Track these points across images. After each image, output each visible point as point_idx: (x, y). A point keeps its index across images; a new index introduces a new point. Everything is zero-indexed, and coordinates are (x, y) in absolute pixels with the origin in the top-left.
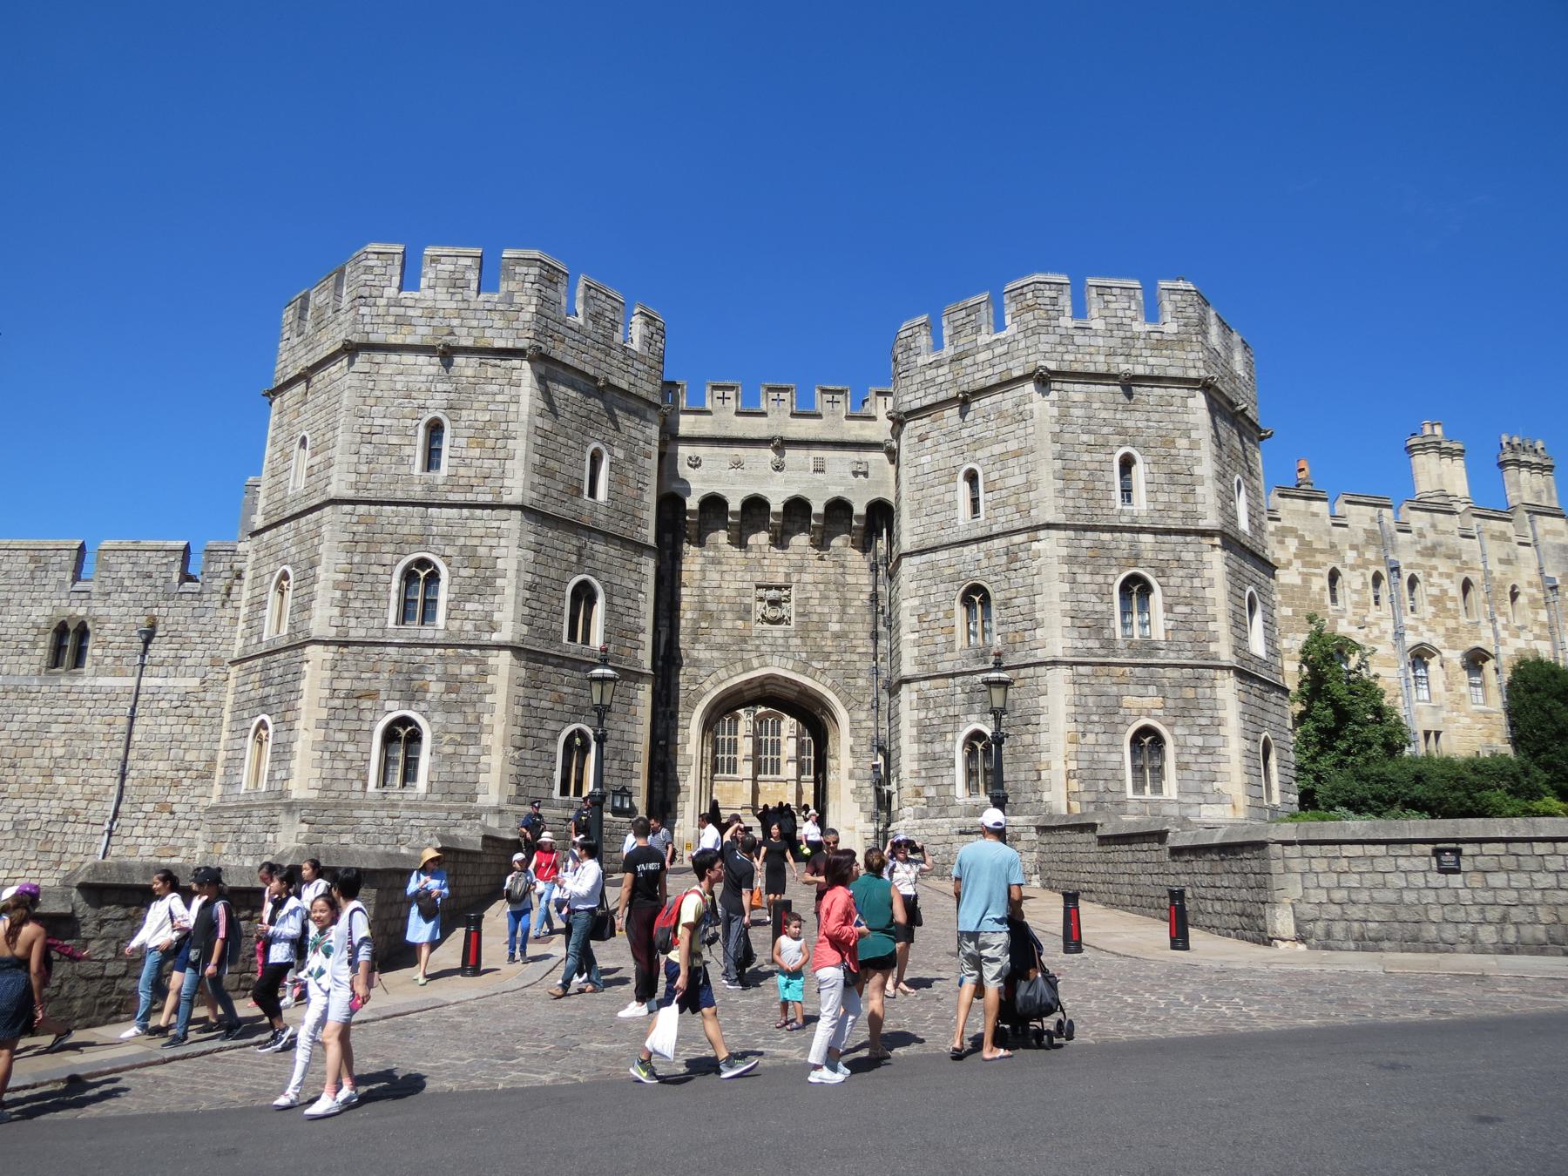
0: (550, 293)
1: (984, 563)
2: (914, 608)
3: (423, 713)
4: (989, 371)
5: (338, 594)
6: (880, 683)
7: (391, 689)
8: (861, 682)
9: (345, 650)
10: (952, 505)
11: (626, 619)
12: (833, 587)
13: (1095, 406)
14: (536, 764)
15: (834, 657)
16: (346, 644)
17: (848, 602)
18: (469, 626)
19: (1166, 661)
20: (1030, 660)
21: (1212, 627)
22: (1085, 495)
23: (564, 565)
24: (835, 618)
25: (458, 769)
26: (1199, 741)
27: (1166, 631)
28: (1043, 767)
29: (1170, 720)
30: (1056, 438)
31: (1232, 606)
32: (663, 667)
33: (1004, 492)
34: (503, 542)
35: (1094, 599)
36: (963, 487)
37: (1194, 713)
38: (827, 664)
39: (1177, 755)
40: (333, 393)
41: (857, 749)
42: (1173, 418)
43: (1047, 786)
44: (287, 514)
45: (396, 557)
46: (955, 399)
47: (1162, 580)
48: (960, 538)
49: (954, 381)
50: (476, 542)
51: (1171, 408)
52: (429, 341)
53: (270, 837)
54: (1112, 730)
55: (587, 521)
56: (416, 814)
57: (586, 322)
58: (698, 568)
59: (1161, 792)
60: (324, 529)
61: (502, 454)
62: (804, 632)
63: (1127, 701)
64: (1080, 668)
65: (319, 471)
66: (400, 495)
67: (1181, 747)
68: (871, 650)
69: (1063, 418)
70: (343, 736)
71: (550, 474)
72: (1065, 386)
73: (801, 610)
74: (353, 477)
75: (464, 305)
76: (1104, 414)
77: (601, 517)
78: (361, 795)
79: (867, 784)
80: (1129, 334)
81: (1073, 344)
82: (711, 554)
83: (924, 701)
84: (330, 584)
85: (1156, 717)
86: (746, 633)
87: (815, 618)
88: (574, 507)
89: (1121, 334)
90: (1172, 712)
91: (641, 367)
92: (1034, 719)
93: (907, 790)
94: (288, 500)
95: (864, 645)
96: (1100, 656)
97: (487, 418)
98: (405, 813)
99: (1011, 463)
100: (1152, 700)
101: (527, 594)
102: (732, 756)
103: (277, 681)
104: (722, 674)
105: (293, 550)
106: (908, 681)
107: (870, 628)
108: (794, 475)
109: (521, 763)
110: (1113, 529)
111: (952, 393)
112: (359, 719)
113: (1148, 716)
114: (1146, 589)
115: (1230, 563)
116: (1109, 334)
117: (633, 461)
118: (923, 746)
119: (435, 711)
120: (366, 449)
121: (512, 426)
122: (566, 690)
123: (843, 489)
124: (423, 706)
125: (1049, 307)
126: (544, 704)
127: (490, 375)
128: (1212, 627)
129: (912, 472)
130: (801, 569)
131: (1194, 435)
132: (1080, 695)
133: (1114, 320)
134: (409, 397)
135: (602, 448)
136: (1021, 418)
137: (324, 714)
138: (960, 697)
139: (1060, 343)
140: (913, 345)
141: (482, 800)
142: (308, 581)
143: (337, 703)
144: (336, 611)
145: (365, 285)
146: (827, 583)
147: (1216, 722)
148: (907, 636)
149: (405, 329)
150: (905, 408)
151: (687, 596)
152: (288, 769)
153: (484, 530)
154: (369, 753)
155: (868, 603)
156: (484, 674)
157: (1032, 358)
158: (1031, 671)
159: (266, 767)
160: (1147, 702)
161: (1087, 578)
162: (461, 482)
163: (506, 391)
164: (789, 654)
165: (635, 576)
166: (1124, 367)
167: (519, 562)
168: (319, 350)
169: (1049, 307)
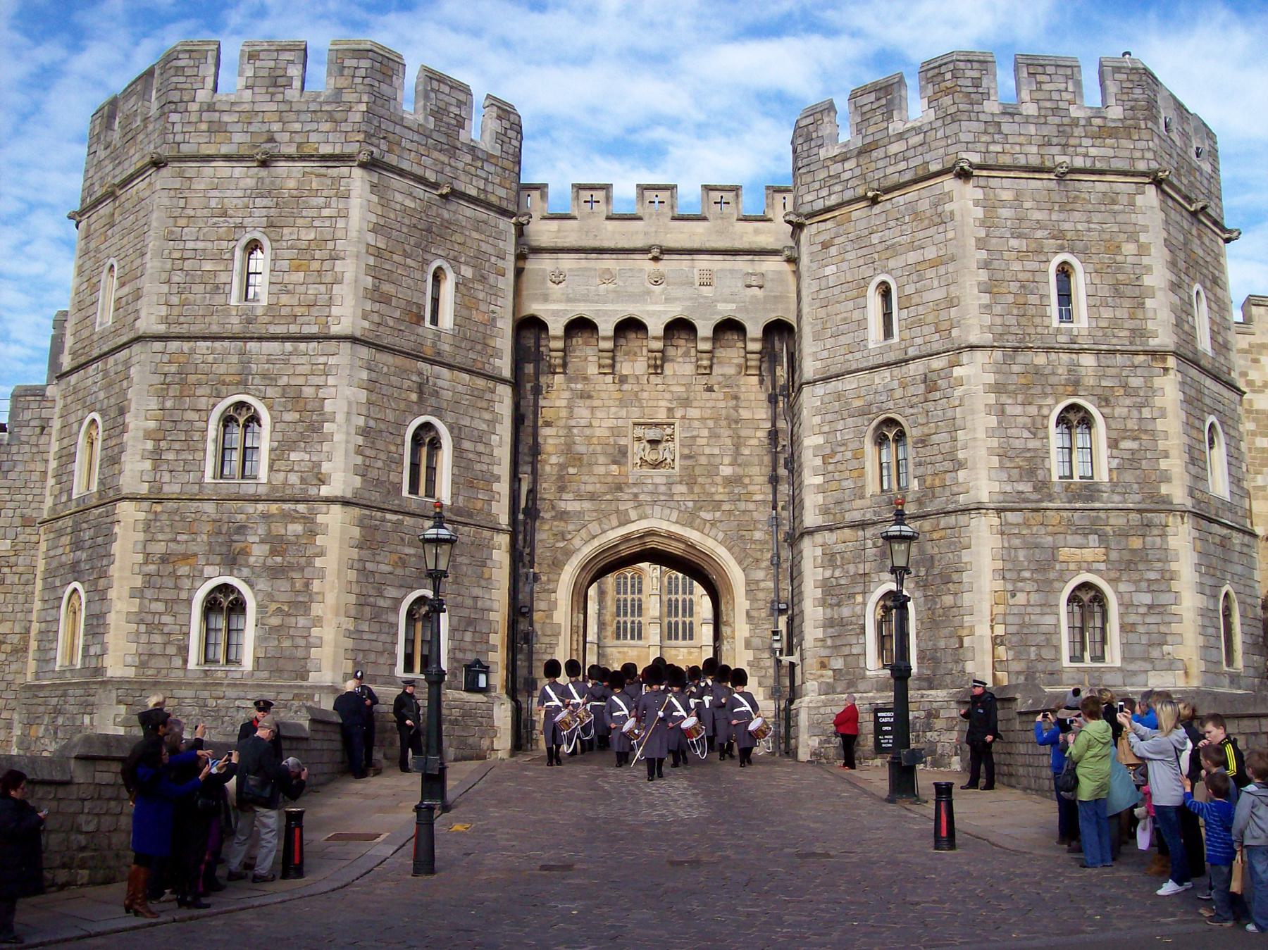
0: (385, 88)
1: (898, 393)
2: (817, 447)
3: (246, 581)
4: (902, 165)
5: (149, 445)
6: (781, 537)
7: (211, 551)
8: (758, 535)
9: (158, 508)
10: (862, 324)
11: (478, 467)
12: (724, 423)
13: (1026, 205)
14: (374, 637)
15: (726, 507)
16: (160, 501)
17: (742, 440)
18: (294, 478)
19: (1110, 506)
20: (951, 507)
21: (1163, 464)
22: (1015, 312)
23: (403, 405)
24: (727, 460)
25: (287, 643)
26: (1146, 599)
27: (1110, 470)
28: (965, 632)
29: (1113, 575)
30: (981, 244)
31: (1186, 440)
32: (525, 520)
33: (920, 308)
34: (331, 381)
35: (1026, 434)
36: (874, 302)
37: (1141, 566)
38: (718, 514)
39: (1121, 615)
40: (142, 213)
41: (754, 613)
42: (1120, 218)
43: (970, 655)
44: (95, 353)
45: (212, 401)
46: (864, 198)
47: (1106, 410)
48: (870, 364)
49: (863, 176)
50: (301, 381)
51: (1116, 207)
52: (244, 151)
53: (87, 719)
54: (1047, 587)
55: (429, 352)
56: (242, 694)
57: (426, 119)
58: (563, 403)
59: (1102, 658)
60: (133, 370)
61: (328, 278)
62: (690, 480)
63: (1064, 553)
64: (1009, 514)
65: (128, 304)
66: (215, 329)
67: (1126, 606)
68: (770, 498)
69: (988, 222)
70: (159, 607)
71: (385, 299)
72: (993, 182)
73: (686, 452)
74: (164, 311)
75: (287, 107)
76: (1038, 215)
77: (446, 348)
78: (181, 673)
79: (766, 655)
80: (1066, 121)
81: (1000, 132)
82: (579, 386)
83: (830, 558)
84: (141, 434)
85: (1097, 572)
86: (622, 480)
87: (703, 460)
88: (412, 338)
89: (1057, 120)
90: (1117, 565)
91: (492, 169)
92: (955, 577)
93: (811, 662)
94: (95, 337)
95: (761, 491)
96: (1033, 501)
97: (312, 236)
98: (231, 693)
99: (930, 273)
100: (1093, 552)
101: (360, 440)
102: (637, 619)
103: (87, 544)
104: (594, 528)
106: (811, 532)
107: (767, 470)
108: (677, 292)
109: (356, 634)
110: (1048, 350)
111: (860, 191)
112: (176, 587)
113: (1089, 571)
115: (1187, 390)
116: (1043, 120)
117: (483, 279)
118: (828, 611)
119: (259, 576)
120: (178, 277)
123: (733, 306)
124: (246, 572)
125: (971, 90)
126: (385, 568)
127: (314, 186)
128: (1163, 464)
130: (686, 402)
131: (1143, 238)
132: (1010, 547)
133: (1048, 104)
134: (224, 214)
135: (445, 265)
136: (941, 220)
137: (138, 582)
139: (985, 132)
140: (814, 135)
141: (314, 678)
142: (118, 431)
143: (152, 568)
144: (148, 465)
145: (176, 89)
146: (716, 420)
147: (1167, 576)
148: (811, 479)
149: (220, 137)
150: (806, 209)
151: (550, 438)
152: (103, 644)
153: (309, 367)
154: (188, 625)
155: (766, 441)
156: (312, 534)
157: (952, 150)
158: (951, 520)
159: (80, 642)
160: (1088, 554)
161: (1018, 410)
162: (284, 311)
163: (334, 205)
164: (672, 504)
165: (487, 416)
166: (1059, 159)
167: (350, 403)
168: (126, 164)
169: (971, 90)
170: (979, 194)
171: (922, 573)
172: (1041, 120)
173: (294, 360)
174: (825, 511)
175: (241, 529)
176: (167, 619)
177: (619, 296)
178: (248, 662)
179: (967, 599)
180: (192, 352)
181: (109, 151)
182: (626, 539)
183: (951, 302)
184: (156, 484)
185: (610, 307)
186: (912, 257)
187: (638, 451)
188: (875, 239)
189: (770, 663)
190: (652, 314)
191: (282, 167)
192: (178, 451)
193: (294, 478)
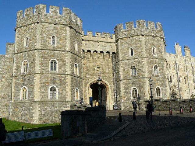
5: (40, 66)
6: (114, 81)
8: (112, 81)
16: (42, 74)
18: (62, 71)
25: (63, 95)
26: (164, 89)
30: (145, 45)
49: (128, 34)
50: (62, 57)
53: (31, 107)
61: (65, 42)
66: (49, 49)
67: (162, 90)
69: (146, 42)
70: (44, 90)
76: (151, 42)
83: (125, 84)
84: (38, 64)
87: (104, 70)
93: (122, 97)
95: (112, 75)
98: (55, 102)
104: (91, 79)
105: (28, 57)
106: (122, 80)
110: (153, 58)
111: (128, 36)
114: (157, 68)
121: (66, 38)
122: (75, 82)
123: (108, 50)
129: (121, 48)
130: (102, 62)
134: (49, 31)
136: (140, 41)
137: (40, 86)
138: (131, 83)
141: (67, 100)
144: (40, 69)
149: (48, 20)
154: (48, 93)
156: (65, 79)
166: (153, 35)
168: (29, 22)
170: (144, 38)
171: (139, 85)
172: (151, 29)
173: (61, 54)
174: (124, 77)
175: (55, 79)
176: (44, 92)
177: (94, 47)
178: (57, 98)
179: (145, 89)
180: (46, 52)
181: (23, 19)
182: (95, 81)
183: (142, 52)
184: (42, 72)
185: (93, 49)
186: (136, 45)
187: (96, 69)
188: (130, 43)
189: (114, 98)
190: (98, 50)
191: (57, 25)
192: (45, 67)
193: (62, 71)
